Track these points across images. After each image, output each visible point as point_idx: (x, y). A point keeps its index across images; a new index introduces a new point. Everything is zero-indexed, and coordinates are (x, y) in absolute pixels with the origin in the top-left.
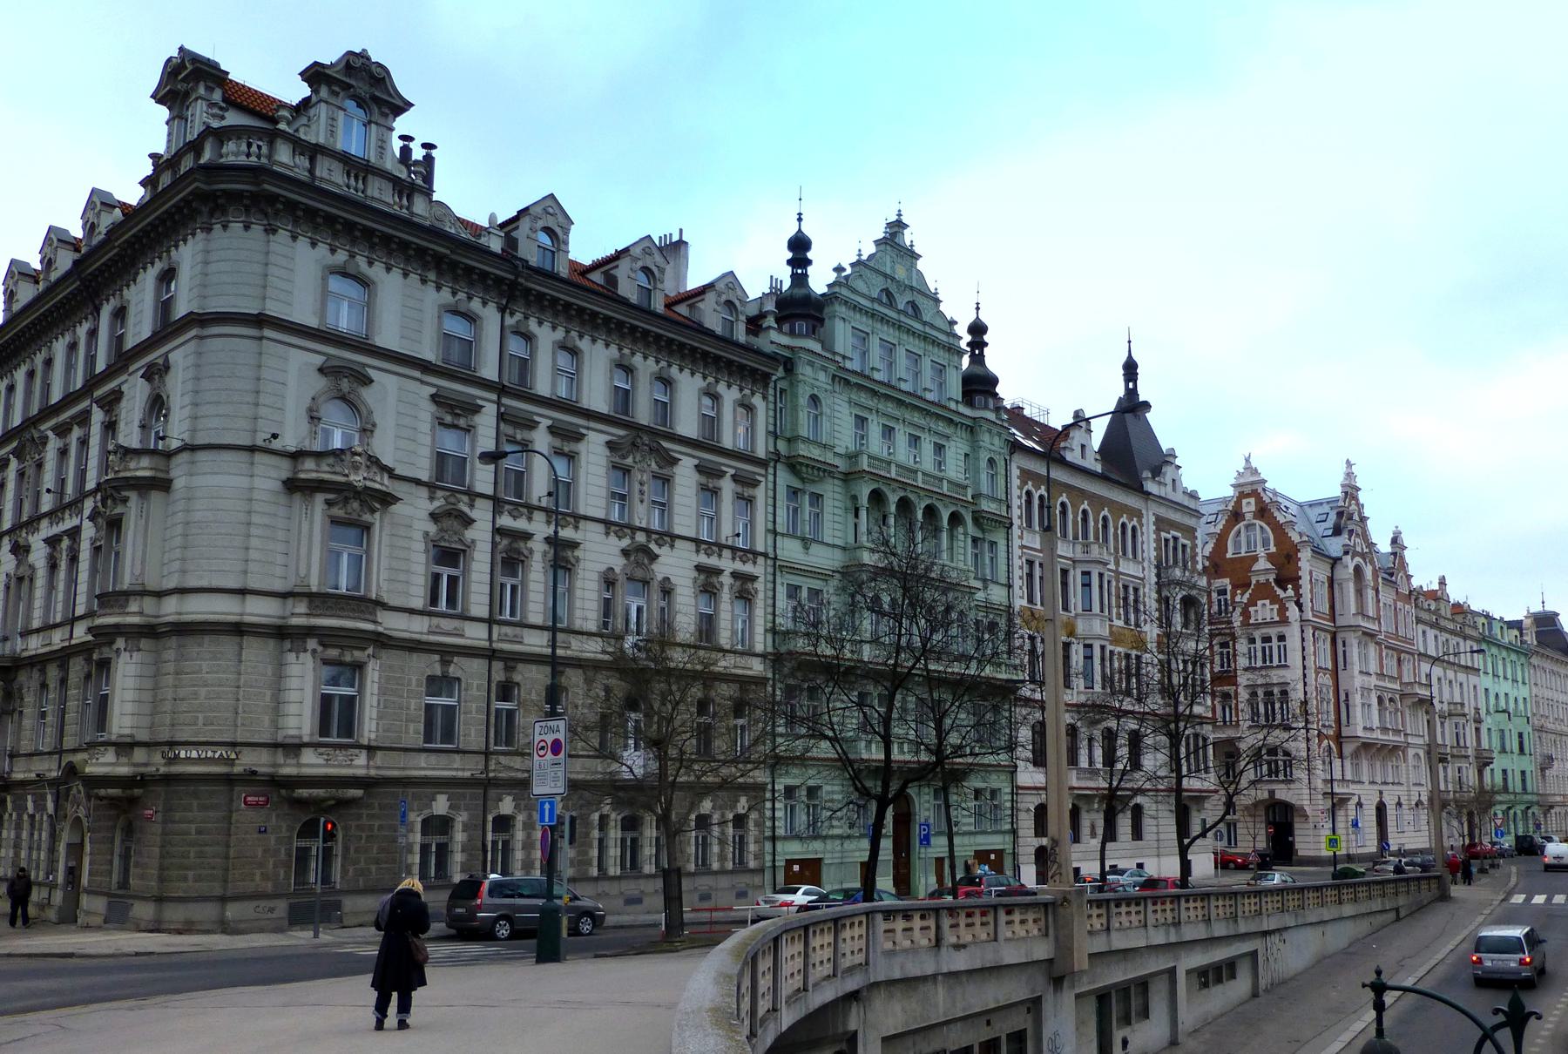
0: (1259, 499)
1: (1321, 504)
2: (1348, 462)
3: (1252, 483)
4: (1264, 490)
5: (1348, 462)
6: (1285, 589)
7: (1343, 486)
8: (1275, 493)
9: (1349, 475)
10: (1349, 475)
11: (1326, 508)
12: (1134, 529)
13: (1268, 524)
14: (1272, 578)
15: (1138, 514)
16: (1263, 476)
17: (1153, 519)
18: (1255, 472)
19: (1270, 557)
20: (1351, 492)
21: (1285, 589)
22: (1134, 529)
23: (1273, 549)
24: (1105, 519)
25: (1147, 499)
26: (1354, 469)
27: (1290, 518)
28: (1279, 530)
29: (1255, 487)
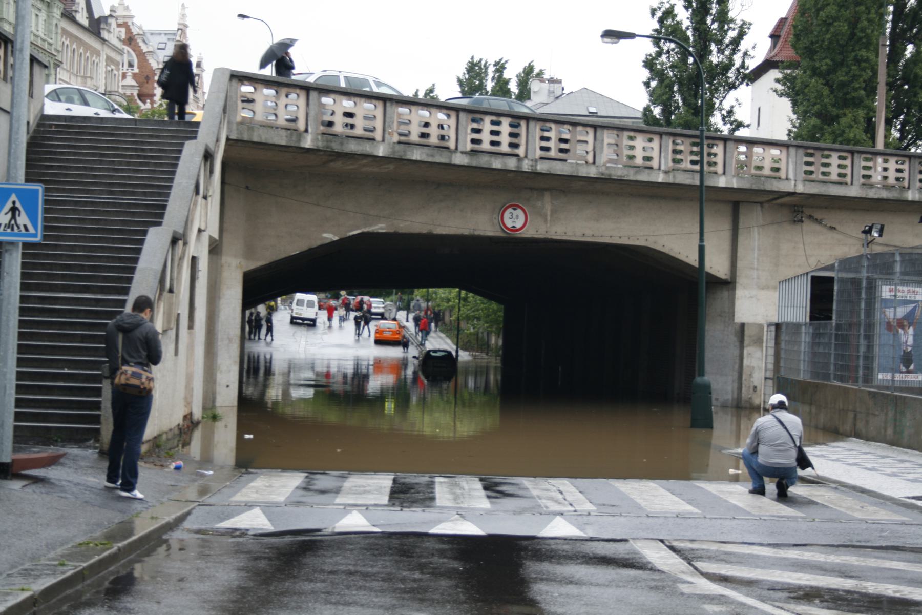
0: (128, 30)
1: (160, 34)
2: (183, 5)
3: (124, 17)
4: (133, 23)
5: (183, 5)
6: (145, 103)
7: (179, 24)
8: (140, 28)
9: (184, 16)
10: (184, 16)
11: (164, 39)
12: (97, 64)
13: (134, 51)
14: (135, 93)
15: (98, 54)
16: (133, 13)
17: (105, 57)
18: (127, 8)
19: (135, 76)
20: (182, 29)
21: (145, 103)
22: (97, 64)
23: (136, 70)
24: (74, 49)
25: (103, 44)
26: (187, 11)
27: (151, 49)
28: (142, 56)
29: (126, 20)
